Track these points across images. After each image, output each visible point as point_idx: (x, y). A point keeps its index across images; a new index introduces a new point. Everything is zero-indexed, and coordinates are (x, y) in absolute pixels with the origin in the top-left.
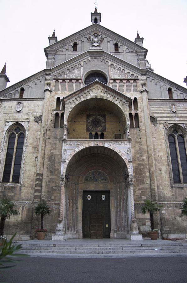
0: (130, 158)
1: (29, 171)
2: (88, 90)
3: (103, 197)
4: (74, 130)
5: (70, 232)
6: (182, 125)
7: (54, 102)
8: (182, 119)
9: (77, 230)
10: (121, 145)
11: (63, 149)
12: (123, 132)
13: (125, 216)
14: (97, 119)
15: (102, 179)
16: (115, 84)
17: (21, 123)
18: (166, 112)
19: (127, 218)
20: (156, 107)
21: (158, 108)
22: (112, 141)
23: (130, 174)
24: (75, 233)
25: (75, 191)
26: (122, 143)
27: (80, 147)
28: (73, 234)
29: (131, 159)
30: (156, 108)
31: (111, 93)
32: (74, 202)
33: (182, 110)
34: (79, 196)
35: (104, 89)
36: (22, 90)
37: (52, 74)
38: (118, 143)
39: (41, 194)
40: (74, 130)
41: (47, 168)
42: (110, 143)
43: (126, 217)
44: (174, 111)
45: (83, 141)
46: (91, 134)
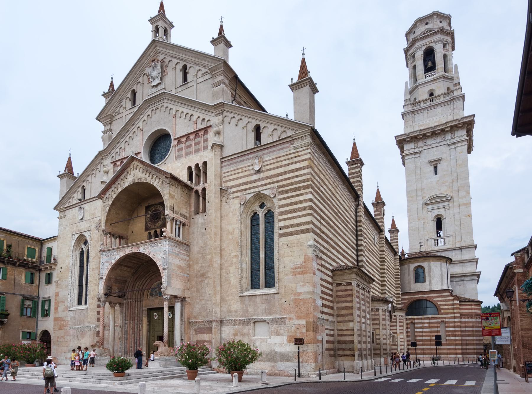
0: (165, 264)
6: (267, 192)
8: (269, 181)
10: (157, 247)
11: (101, 262)
18: (246, 173)
20: (232, 169)
21: (235, 170)
22: (147, 244)
26: (158, 244)
29: (166, 265)
30: (232, 171)
33: (272, 163)
37: (109, 156)
38: (153, 245)
42: (145, 247)
44: (257, 169)
45: (118, 249)
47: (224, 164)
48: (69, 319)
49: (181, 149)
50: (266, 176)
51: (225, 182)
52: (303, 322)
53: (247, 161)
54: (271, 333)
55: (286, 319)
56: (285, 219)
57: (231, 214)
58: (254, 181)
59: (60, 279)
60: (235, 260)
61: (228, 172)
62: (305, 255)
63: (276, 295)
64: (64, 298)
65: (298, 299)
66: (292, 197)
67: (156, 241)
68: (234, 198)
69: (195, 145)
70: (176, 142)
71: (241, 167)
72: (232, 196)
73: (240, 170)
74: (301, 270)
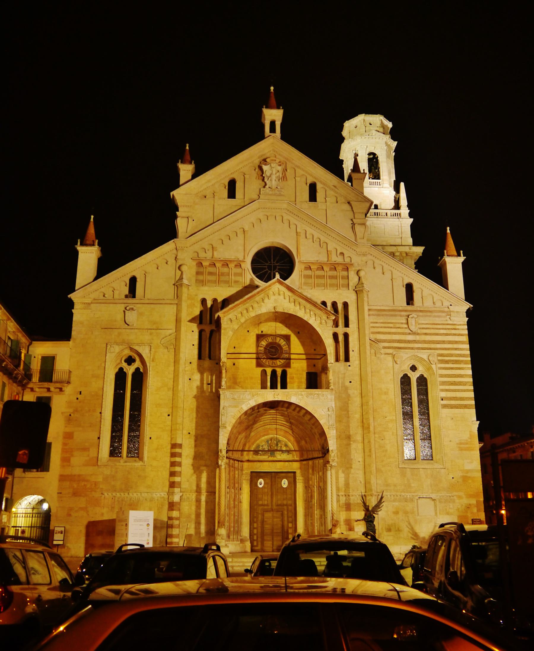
1: (157, 438)
2: (262, 295)
3: (285, 483)
4: (234, 364)
5: (231, 542)
7: (195, 309)
8: (426, 346)
9: (241, 538)
10: (318, 400)
12: (321, 369)
13: (321, 515)
14: (276, 343)
15: (283, 451)
16: (309, 272)
17: (136, 348)
18: (399, 330)
19: (324, 519)
20: (381, 321)
21: (385, 323)
22: (303, 393)
23: (330, 449)
24: (239, 542)
25: (237, 472)
27: (250, 402)
28: (236, 545)
30: (381, 323)
31: (303, 302)
32: (237, 491)
34: (244, 482)
35: (290, 294)
36: (133, 281)
39: (181, 479)
40: (234, 364)
41: (189, 433)
42: (300, 397)
43: (323, 516)
46: (264, 373)
47: (371, 313)
48: (100, 479)
49: (310, 277)
50: (423, 339)
51: (373, 333)
52: (473, 501)
53: (399, 318)
54: (440, 513)
55: (455, 497)
56: (447, 390)
57: (383, 372)
58: (409, 342)
59: (76, 411)
60: (390, 425)
61: (377, 323)
62: (470, 432)
63: (443, 470)
64: (87, 444)
65: (466, 476)
66: (452, 368)
67: (316, 392)
68: (386, 354)
69: (329, 278)
70: (303, 267)
71: (393, 321)
72: (383, 351)
73: (391, 325)
74: (467, 446)
